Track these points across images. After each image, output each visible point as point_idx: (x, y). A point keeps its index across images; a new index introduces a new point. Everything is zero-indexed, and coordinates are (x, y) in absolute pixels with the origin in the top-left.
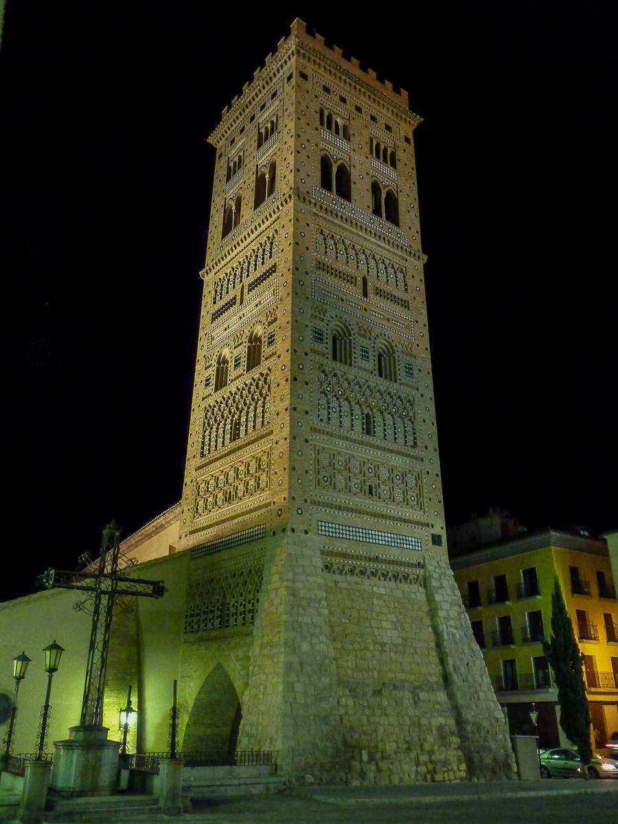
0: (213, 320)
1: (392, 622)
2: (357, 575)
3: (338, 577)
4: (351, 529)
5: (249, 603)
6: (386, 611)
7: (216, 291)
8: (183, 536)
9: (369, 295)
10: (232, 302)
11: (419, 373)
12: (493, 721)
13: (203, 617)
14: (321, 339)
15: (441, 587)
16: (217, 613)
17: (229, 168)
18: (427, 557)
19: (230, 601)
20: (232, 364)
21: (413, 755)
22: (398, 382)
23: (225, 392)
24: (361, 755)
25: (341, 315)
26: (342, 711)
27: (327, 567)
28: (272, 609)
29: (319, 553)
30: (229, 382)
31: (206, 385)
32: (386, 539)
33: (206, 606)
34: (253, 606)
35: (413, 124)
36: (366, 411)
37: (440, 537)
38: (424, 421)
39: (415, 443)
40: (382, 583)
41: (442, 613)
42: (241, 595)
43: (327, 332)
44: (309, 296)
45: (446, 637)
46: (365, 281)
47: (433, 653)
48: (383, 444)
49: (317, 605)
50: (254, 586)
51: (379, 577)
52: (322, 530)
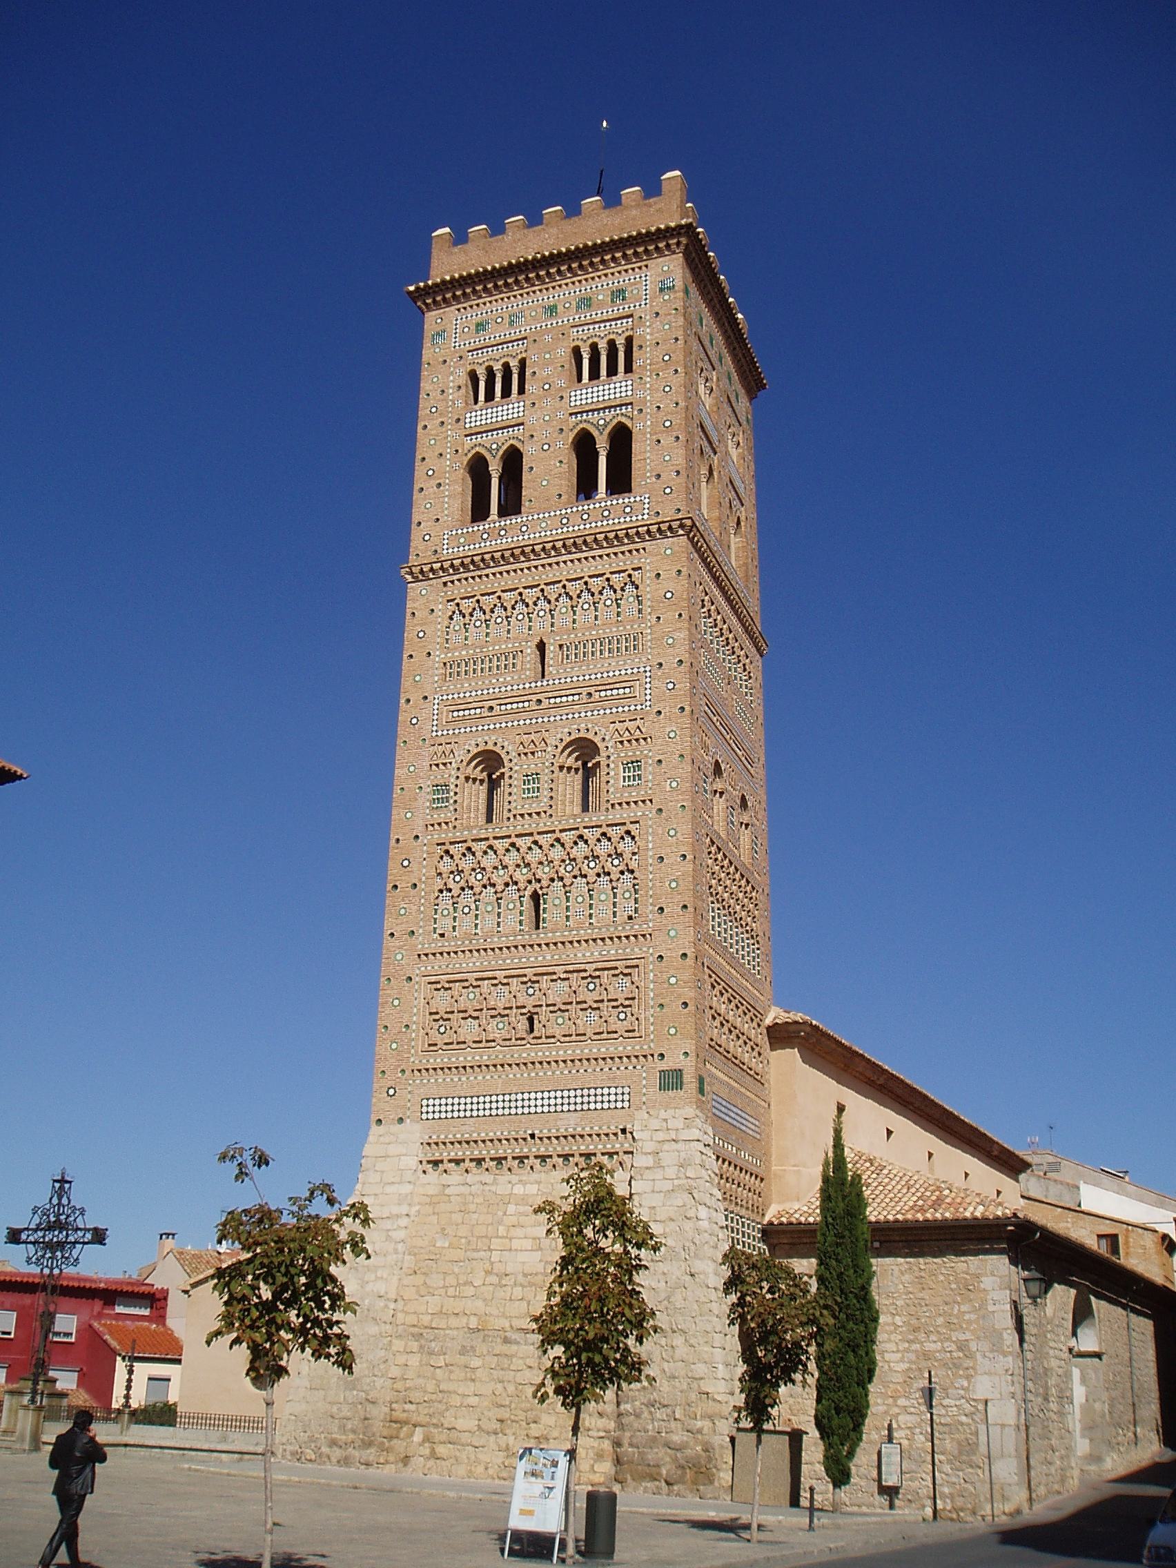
3: (455, 1176)
12: (693, 1396)
15: (659, 1165)
21: (502, 1440)
22: (603, 808)
25: (486, 738)
26: (395, 1372)
32: (552, 1102)
35: (678, 244)
36: (530, 889)
38: (662, 858)
39: (636, 910)
40: (535, 1176)
43: (458, 782)
44: (427, 737)
46: (541, 647)
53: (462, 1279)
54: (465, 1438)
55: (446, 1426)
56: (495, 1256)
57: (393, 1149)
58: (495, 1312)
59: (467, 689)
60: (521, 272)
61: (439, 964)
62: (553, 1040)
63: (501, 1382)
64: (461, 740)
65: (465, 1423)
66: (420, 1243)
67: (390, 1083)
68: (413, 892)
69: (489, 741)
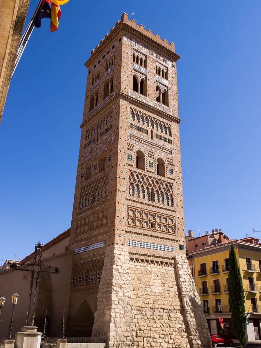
0: (85, 147)
1: (160, 283)
2: (145, 263)
3: (136, 264)
4: (142, 243)
5: (98, 274)
6: (157, 278)
7: (87, 135)
8: (71, 244)
9: (154, 138)
10: (93, 141)
11: (176, 173)
13: (79, 280)
14: (131, 159)
16: (85, 278)
17: (93, 79)
18: (176, 255)
19: (90, 273)
20: (93, 168)
21: (166, 340)
22: (166, 177)
23: (89, 181)
24: (144, 340)
26: (136, 321)
27: (132, 259)
28: (107, 278)
29: (127, 254)
30: (91, 176)
31: (82, 177)
32: (158, 247)
33: (80, 275)
34: (100, 276)
37: (183, 246)
40: (156, 266)
41: (182, 280)
42: (95, 271)
45: (183, 290)
46: (152, 132)
47: (177, 296)
48: (158, 205)
49: (127, 276)
50: (100, 267)
51: (155, 264)
52: (129, 244)
53: (146, 293)
54: (157, 339)
55: (152, 337)
56: (152, 287)
57: (122, 253)
58: (156, 303)
59: (136, 133)
60: (147, 39)
61: (131, 203)
62: (158, 231)
63: (162, 323)
64: (135, 145)
65: (157, 336)
66: (133, 282)
67: (120, 233)
68: (124, 181)
69: (142, 149)
